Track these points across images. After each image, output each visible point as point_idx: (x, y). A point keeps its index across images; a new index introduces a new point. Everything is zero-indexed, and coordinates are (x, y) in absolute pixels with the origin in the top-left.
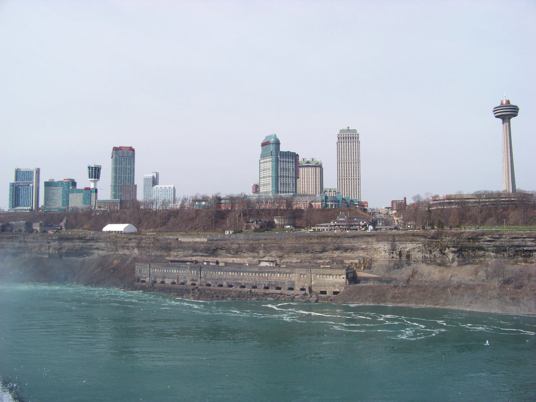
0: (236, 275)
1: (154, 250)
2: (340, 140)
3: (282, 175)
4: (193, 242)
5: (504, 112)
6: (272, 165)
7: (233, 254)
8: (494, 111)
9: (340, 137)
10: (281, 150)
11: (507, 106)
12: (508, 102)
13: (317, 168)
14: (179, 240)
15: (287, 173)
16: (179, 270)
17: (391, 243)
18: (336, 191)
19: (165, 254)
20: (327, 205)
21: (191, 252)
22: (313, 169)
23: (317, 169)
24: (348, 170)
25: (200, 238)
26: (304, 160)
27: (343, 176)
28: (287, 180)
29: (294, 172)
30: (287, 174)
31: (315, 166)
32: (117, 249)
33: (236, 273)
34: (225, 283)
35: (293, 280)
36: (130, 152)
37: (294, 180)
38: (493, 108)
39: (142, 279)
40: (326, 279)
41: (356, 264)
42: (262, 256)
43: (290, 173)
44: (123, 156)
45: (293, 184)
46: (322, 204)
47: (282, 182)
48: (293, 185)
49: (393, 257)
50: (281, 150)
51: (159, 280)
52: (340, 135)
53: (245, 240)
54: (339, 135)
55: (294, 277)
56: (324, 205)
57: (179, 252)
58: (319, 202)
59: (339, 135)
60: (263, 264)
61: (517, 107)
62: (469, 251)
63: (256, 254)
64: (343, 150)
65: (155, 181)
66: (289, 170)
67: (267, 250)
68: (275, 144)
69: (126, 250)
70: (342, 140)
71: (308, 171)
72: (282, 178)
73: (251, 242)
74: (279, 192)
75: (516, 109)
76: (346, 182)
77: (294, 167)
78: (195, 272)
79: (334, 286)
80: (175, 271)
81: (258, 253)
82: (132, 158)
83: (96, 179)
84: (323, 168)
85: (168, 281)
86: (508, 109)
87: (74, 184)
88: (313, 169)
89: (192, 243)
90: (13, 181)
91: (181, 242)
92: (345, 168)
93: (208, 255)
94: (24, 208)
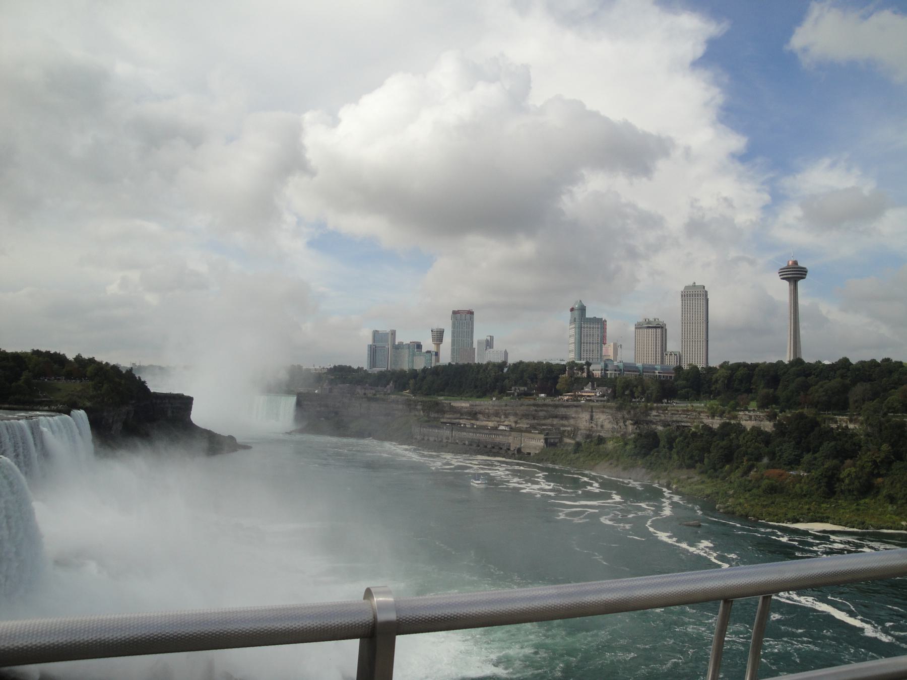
3: (585, 341)
6: (575, 332)
8: (780, 276)
10: (586, 317)
11: (793, 268)
12: (795, 263)
14: (451, 404)
17: (590, 413)
19: (441, 416)
20: (606, 374)
21: (458, 415)
22: (653, 330)
24: (686, 331)
27: (686, 338)
28: (591, 347)
29: (599, 338)
31: (656, 327)
34: (467, 443)
35: (510, 442)
37: (599, 346)
38: (779, 269)
39: (415, 437)
40: (531, 442)
42: (503, 420)
43: (594, 339)
45: (598, 350)
46: (601, 373)
47: (585, 349)
48: (598, 352)
49: (592, 427)
56: (603, 373)
58: (599, 371)
60: (502, 428)
61: (805, 268)
63: (498, 419)
64: (699, 307)
65: (489, 344)
67: (506, 416)
68: (580, 309)
71: (648, 332)
72: (585, 345)
73: (496, 408)
75: (805, 271)
76: (701, 344)
77: (600, 334)
79: (536, 449)
81: (500, 417)
84: (666, 330)
85: (432, 439)
87: (419, 346)
88: (653, 330)
90: (371, 343)
91: (452, 406)
92: (686, 329)
94: (376, 370)
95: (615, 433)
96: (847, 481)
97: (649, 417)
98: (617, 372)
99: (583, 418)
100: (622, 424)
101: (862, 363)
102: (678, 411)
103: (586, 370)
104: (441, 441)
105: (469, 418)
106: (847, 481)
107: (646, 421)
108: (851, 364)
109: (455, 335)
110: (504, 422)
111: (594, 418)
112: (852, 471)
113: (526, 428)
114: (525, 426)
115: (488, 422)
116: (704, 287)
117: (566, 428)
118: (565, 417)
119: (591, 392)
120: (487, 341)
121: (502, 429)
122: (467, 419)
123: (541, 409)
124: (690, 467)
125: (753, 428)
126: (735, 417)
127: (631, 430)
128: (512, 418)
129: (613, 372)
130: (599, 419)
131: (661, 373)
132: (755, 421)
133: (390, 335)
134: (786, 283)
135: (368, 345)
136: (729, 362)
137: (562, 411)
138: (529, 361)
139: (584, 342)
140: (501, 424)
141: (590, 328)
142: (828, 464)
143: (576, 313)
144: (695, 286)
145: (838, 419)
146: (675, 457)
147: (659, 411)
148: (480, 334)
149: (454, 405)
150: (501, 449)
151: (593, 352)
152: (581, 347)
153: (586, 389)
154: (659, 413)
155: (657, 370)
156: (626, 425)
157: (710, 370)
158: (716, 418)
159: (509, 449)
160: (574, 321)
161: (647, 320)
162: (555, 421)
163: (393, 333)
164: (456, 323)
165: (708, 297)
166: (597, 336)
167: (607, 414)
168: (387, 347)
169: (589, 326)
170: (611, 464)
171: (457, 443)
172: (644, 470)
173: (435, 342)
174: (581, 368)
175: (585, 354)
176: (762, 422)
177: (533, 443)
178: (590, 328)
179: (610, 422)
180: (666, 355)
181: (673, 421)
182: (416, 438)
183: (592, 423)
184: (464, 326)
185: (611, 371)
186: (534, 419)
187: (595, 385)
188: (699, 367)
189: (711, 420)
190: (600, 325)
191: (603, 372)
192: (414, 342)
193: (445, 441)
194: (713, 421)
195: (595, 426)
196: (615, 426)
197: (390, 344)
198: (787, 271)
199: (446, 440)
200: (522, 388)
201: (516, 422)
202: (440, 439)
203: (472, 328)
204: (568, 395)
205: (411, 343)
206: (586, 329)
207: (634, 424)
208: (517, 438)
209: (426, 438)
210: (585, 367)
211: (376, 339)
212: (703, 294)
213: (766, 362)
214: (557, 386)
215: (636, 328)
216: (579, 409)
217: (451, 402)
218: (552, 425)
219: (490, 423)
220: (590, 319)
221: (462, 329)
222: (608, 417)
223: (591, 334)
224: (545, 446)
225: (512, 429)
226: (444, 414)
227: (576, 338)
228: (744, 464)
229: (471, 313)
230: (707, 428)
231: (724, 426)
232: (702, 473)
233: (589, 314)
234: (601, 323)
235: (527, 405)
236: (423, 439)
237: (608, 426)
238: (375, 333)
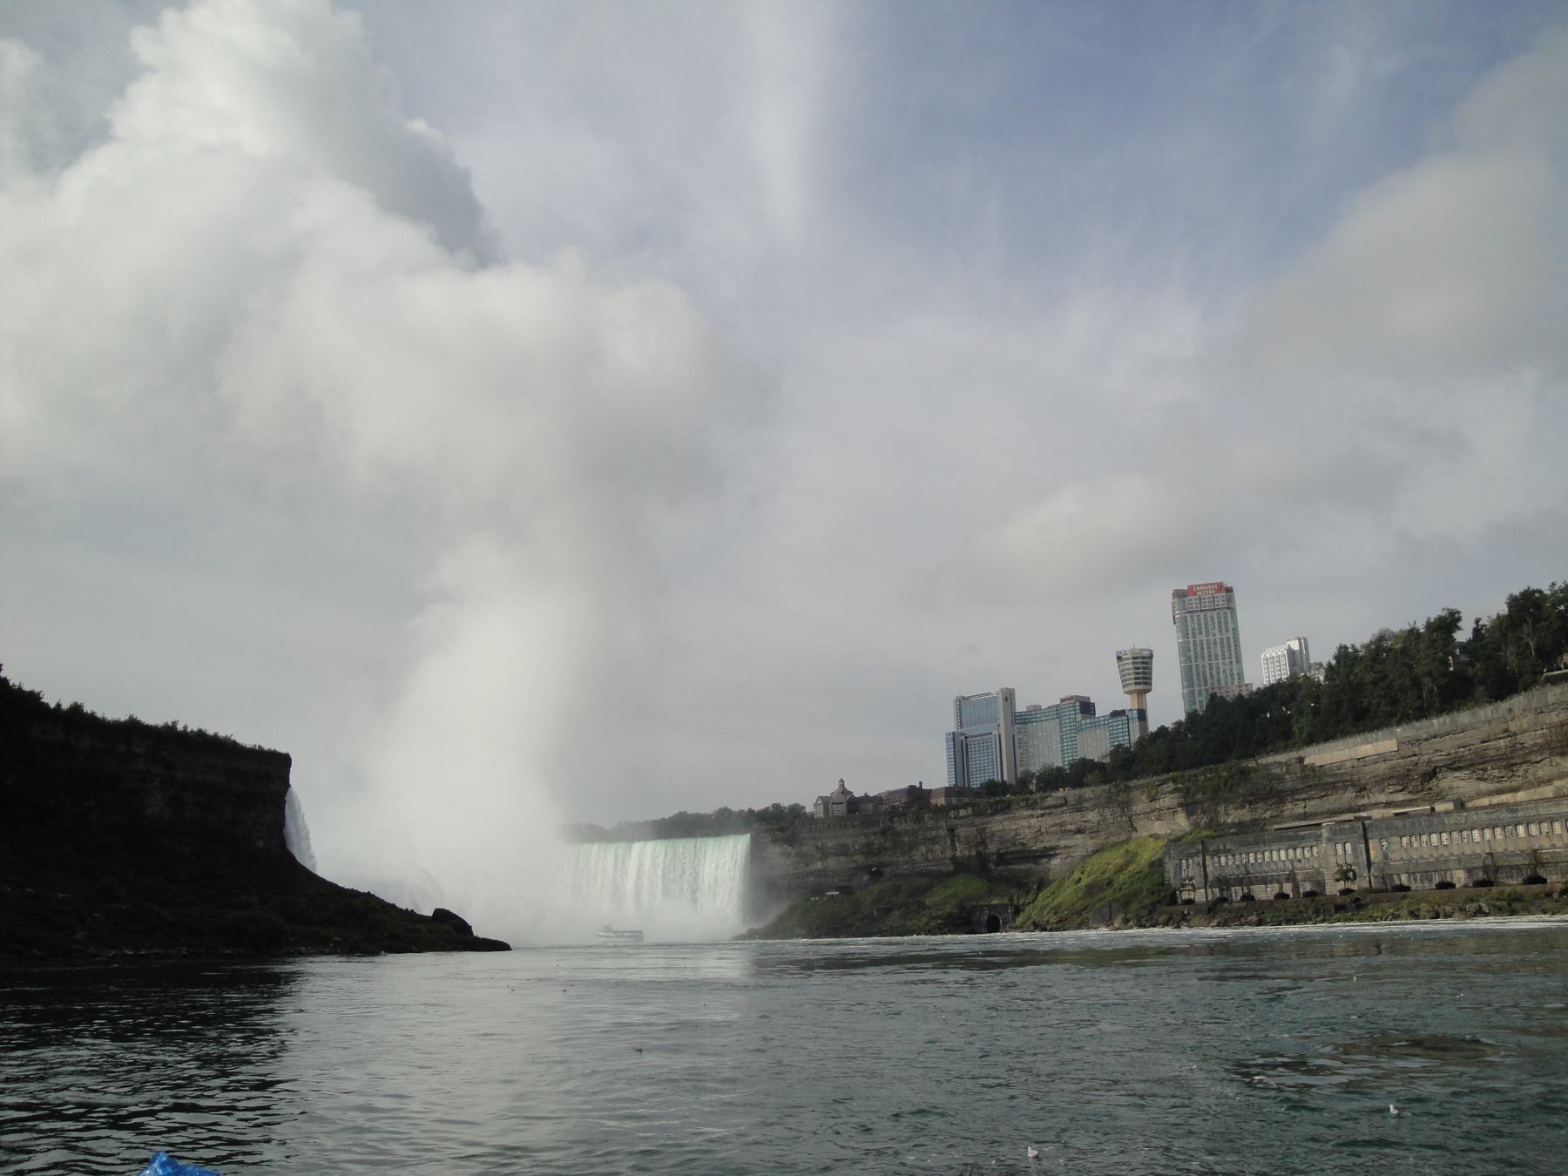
0: (1499, 837)
1: (1231, 806)
7: (1500, 779)
14: (1306, 762)
16: (1295, 849)
21: (1349, 795)
25: (1371, 743)
32: (1132, 825)
33: (1498, 831)
36: (1220, 595)
44: (1202, 611)
51: (1237, 893)
53: (1531, 717)
57: (1312, 802)
69: (1157, 822)
78: (1348, 846)
80: (1283, 853)
82: (1229, 611)
83: (1140, 687)
87: (1087, 707)
89: (1348, 764)
90: (952, 726)
91: (1313, 768)
93: (1408, 797)
105: (1400, 797)
109: (1192, 653)
163: (1009, 696)
197: (1002, 723)
203: (1235, 631)
205: (1063, 700)
211: (964, 719)
217: (1301, 753)
226: (1282, 801)
238: (962, 702)
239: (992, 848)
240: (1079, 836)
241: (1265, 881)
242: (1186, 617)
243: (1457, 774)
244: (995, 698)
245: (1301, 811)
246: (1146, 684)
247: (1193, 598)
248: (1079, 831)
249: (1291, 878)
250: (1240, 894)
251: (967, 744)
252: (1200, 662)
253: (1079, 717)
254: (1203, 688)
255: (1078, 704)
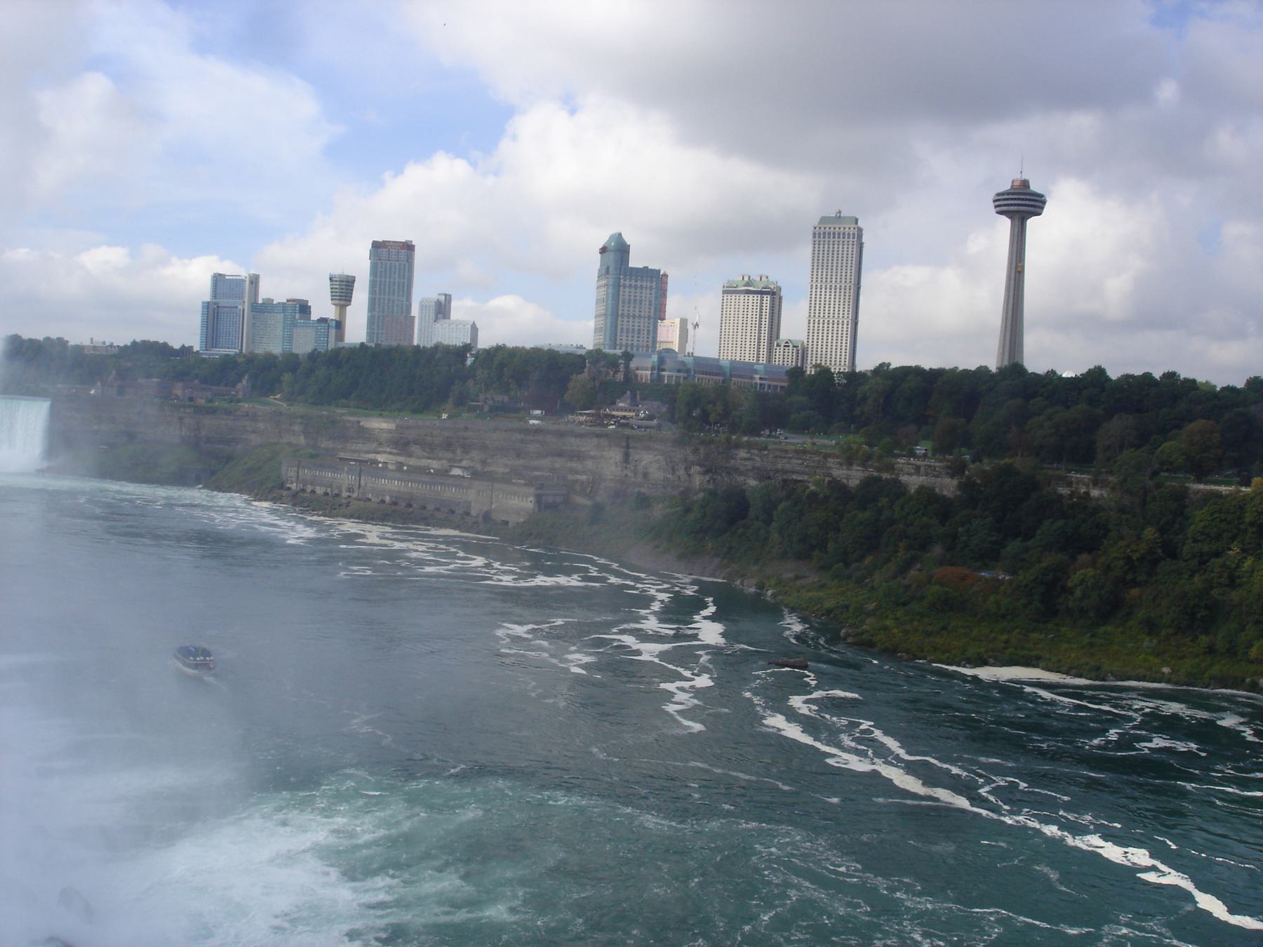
2: (817, 239)
3: (626, 313)
4: (378, 429)
5: (1026, 205)
6: (607, 294)
9: (817, 233)
10: (630, 266)
11: (1019, 194)
12: (1025, 184)
13: (765, 296)
14: (361, 424)
15: (637, 309)
17: (623, 450)
18: (798, 347)
19: (340, 447)
20: (660, 378)
21: (375, 445)
22: (755, 298)
23: (765, 299)
26: (743, 279)
27: (817, 315)
28: (636, 324)
29: (653, 308)
30: (632, 311)
31: (761, 293)
34: (387, 499)
39: (288, 485)
41: (583, 483)
42: (459, 458)
43: (642, 310)
44: (389, 260)
45: (648, 330)
46: (651, 374)
47: (625, 327)
48: (648, 334)
49: (626, 475)
50: (630, 266)
51: (309, 488)
52: (817, 229)
54: (815, 228)
55: (471, 495)
58: (647, 370)
59: (815, 228)
60: (456, 472)
62: (724, 475)
63: (450, 455)
66: (641, 304)
67: (466, 449)
70: (822, 239)
74: (618, 347)
75: (1037, 201)
80: (330, 474)
81: (454, 452)
84: (780, 298)
86: (1019, 199)
87: (304, 308)
88: (755, 298)
90: (208, 298)
95: (669, 489)
96: (1078, 593)
97: (733, 461)
98: (681, 374)
99: (611, 458)
100: (681, 472)
101: (1127, 378)
102: (786, 451)
103: (622, 368)
104: (337, 495)
105: (395, 451)
106: (1078, 593)
107: (727, 468)
108: (1108, 379)
109: (377, 289)
110: (461, 461)
111: (631, 458)
112: (1090, 574)
113: (503, 473)
114: (501, 470)
115: (430, 461)
116: (856, 221)
117: (579, 477)
118: (578, 456)
119: (630, 411)
120: (439, 303)
121: (457, 474)
122: (390, 453)
123: (532, 438)
124: (803, 556)
125: (921, 489)
126: (890, 468)
127: (698, 483)
128: (475, 454)
129: (675, 374)
130: (641, 461)
131: (765, 379)
132: (926, 476)
133: (247, 283)
134: (1005, 224)
135: (203, 303)
136: (889, 364)
137: (573, 443)
138: (515, 346)
139: (623, 315)
140: (456, 464)
141: (636, 287)
142: (1050, 560)
143: (611, 256)
144: (840, 217)
145: (1073, 479)
146: (775, 536)
147: (752, 451)
148: (423, 290)
149: (366, 426)
150: (453, 512)
151: (639, 333)
152: (617, 324)
153: (621, 405)
154: (752, 454)
155: (757, 374)
156: (689, 475)
157: (854, 377)
158: (855, 467)
159: (468, 514)
160: (605, 272)
161: (746, 279)
162: (558, 463)
163: (255, 280)
164: (379, 266)
165: (863, 240)
166: (647, 303)
167: (656, 453)
168: (240, 307)
169: (633, 283)
170: (657, 547)
171: (370, 500)
172: (717, 561)
173: (337, 302)
174: (613, 363)
175: (624, 338)
176: (939, 480)
177: (515, 502)
178: (636, 287)
179: (659, 469)
180: (778, 345)
181: (777, 471)
182: (289, 489)
183: (626, 468)
184: (395, 273)
185: (670, 371)
186: (518, 456)
187: (638, 396)
188: (833, 370)
189: (845, 472)
190: (654, 283)
191: (656, 372)
192: (294, 300)
193: (345, 494)
194: (850, 472)
195: (633, 475)
196: (670, 476)
197: (246, 300)
198: (1008, 199)
199: (348, 494)
200: (499, 398)
201: (484, 462)
202: (336, 492)
204: (585, 414)
205: (288, 301)
206: (627, 290)
207: (706, 472)
208: (483, 492)
209: (309, 488)
210: (621, 361)
212: (854, 234)
213: (956, 368)
214: (566, 395)
215: (724, 292)
216: (604, 442)
217: (360, 419)
218: (553, 470)
219: (435, 462)
220: (637, 270)
221: (390, 278)
222: (657, 458)
223: (638, 298)
224: (536, 510)
225: (476, 475)
227: (607, 305)
228: (899, 554)
229: (409, 247)
230: (837, 486)
231: (868, 483)
232: (823, 568)
233: (635, 262)
234: (655, 281)
235: (506, 431)
236: (303, 491)
237: (657, 474)
238: (218, 279)
239: (203, 433)
240: (253, 435)
241: (321, 485)
242: (377, 263)
243: (416, 446)
244: (243, 281)
245: (353, 448)
246: (346, 300)
247: (384, 250)
248: (254, 432)
249: (331, 486)
250: (311, 489)
251: (218, 312)
252: (382, 297)
253: (297, 316)
254: (381, 314)
255: (298, 306)
